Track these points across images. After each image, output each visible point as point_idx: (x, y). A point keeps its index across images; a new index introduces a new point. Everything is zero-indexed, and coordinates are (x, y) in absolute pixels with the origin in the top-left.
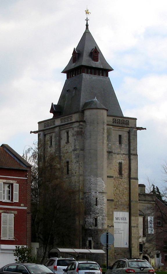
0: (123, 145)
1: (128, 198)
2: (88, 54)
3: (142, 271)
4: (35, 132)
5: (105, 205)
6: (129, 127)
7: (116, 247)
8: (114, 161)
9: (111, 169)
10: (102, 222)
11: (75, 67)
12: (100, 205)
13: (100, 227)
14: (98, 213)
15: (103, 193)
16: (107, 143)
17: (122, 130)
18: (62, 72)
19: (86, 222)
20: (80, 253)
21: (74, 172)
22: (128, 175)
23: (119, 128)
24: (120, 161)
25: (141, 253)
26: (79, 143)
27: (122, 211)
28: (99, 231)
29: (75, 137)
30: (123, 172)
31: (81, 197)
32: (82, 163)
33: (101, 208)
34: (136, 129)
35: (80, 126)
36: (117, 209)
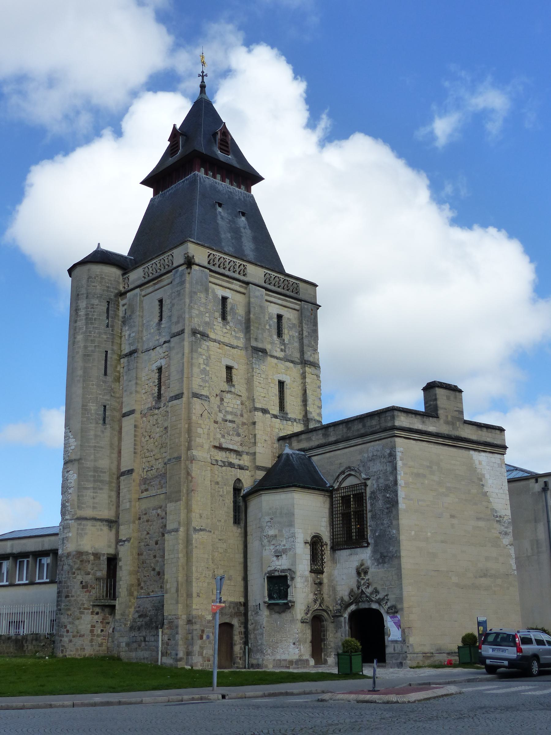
23: (154, 284)
24: (158, 364)
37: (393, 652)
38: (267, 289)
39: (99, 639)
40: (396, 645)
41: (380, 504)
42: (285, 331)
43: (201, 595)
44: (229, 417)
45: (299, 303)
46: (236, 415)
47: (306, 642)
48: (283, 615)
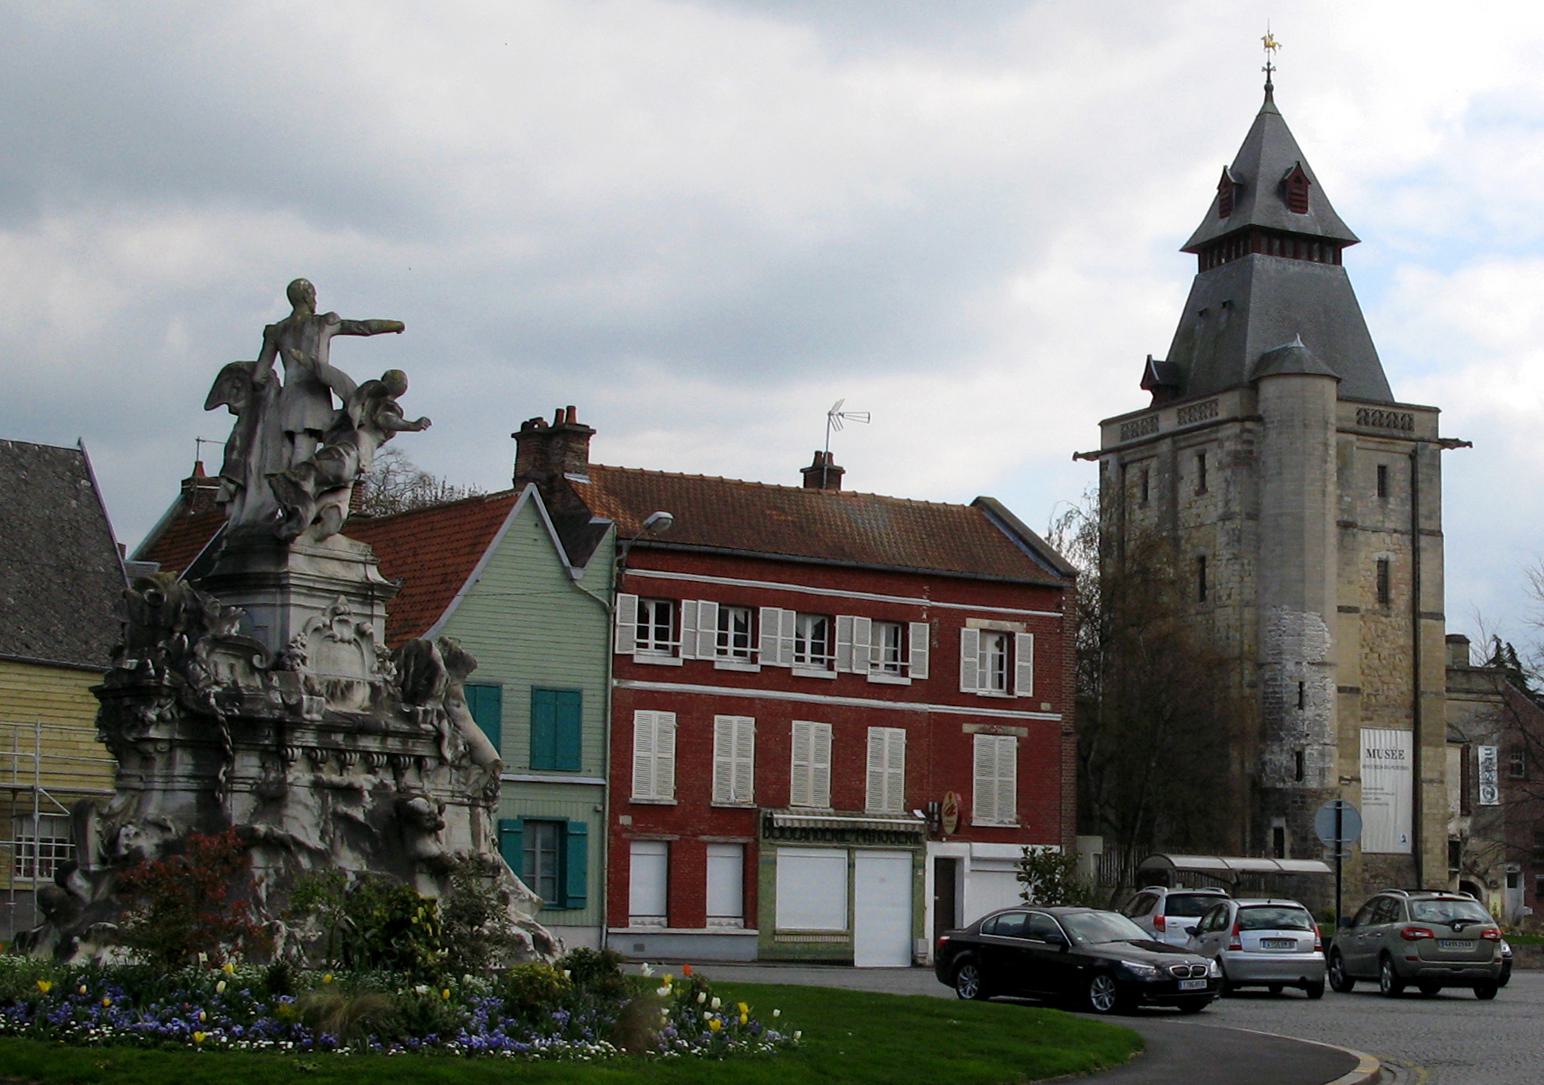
0: (1392, 500)
1: (1411, 682)
2: (1272, 187)
3: (1459, 935)
4: (1089, 456)
5: (1329, 706)
6: (1414, 437)
7: (1368, 850)
8: (1362, 555)
9: (1350, 583)
10: (1321, 765)
11: (1228, 230)
12: (1313, 708)
13: (1312, 783)
14: (1308, 735)
15: (1322, 664)
16: (1339, 492)
17: (1391, 447)
18: (1182, 250)
19: (1264, 764)
20: (1244, 872)
21: (1224, 594)
22: (1411, 602)
23: (1380, 442)
24: (1383, 555)
25: (1456, 873)
26: (1240, 493)
27: (1388, 726)
28: (1312, 797)
29: (1228, 473)
30: (1393, 594)
31: (1248, 678)
32: (1253, 562)
33: (1317, 718)
34: (1437, 446)
35: (1246, 436)
36: (1371, 719)
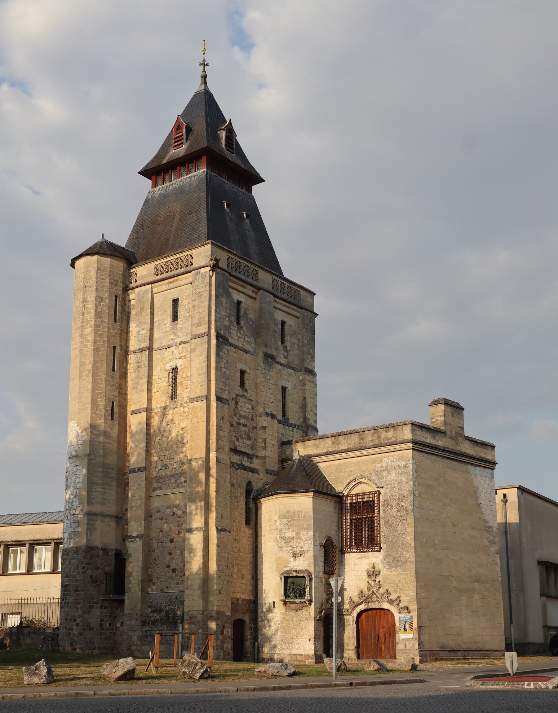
23: (170, 283)
24: (173, 364)
37: (404, 649)
38: (275, 296)
39: (107, 632)
40: (407, 643)
41: (394, 511)
42: (287, 338)
43: (222, 592)
44: (242, 421)
45: (300, 310)
46: (248, 419)
47: (320, 638)
48: (300, 612)
